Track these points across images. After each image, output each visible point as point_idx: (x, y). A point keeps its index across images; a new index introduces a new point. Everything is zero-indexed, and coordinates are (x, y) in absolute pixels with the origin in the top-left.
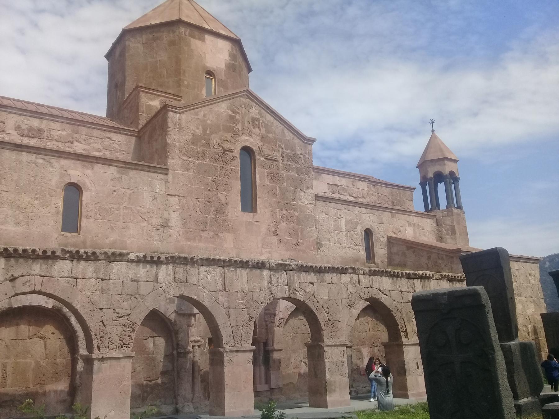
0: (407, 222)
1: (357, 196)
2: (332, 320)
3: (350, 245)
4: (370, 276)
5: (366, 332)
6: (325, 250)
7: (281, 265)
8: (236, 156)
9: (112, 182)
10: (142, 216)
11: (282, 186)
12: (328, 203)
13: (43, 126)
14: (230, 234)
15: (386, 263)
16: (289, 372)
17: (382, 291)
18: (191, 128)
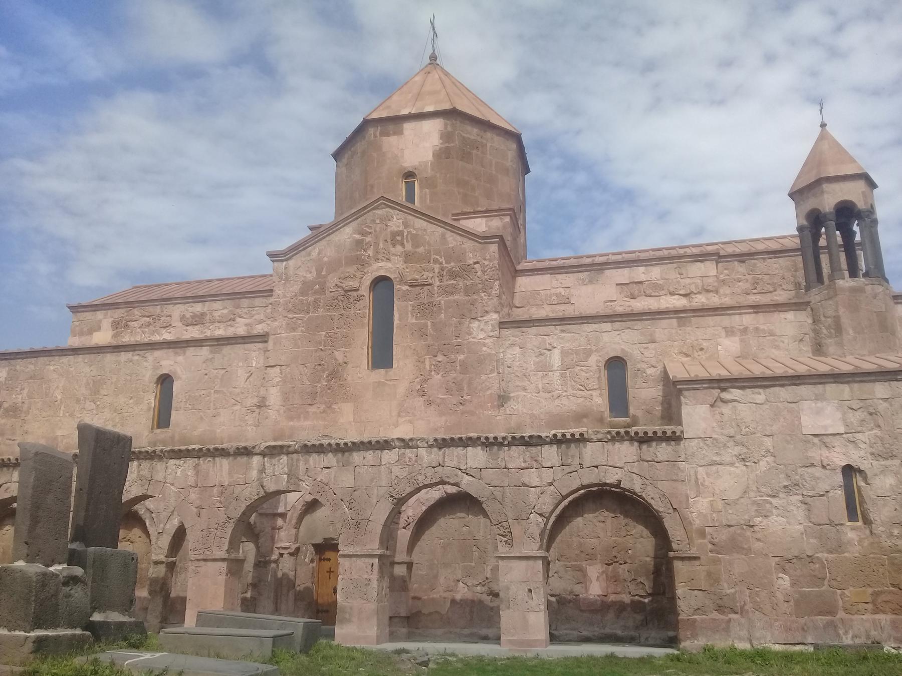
0: (725, 328)
1: (689, 292)
2: (357, 519)
3: (570, 391)
4: (440, 448)
5: (599, 537)
6: (515, 406)
7: (274, 447)
9: (205, 365)
12: (524, 329)
13: (205, 310)
14: (349, 404)
16: (435, 596)
17: (463, 471)
18: (301, 274)
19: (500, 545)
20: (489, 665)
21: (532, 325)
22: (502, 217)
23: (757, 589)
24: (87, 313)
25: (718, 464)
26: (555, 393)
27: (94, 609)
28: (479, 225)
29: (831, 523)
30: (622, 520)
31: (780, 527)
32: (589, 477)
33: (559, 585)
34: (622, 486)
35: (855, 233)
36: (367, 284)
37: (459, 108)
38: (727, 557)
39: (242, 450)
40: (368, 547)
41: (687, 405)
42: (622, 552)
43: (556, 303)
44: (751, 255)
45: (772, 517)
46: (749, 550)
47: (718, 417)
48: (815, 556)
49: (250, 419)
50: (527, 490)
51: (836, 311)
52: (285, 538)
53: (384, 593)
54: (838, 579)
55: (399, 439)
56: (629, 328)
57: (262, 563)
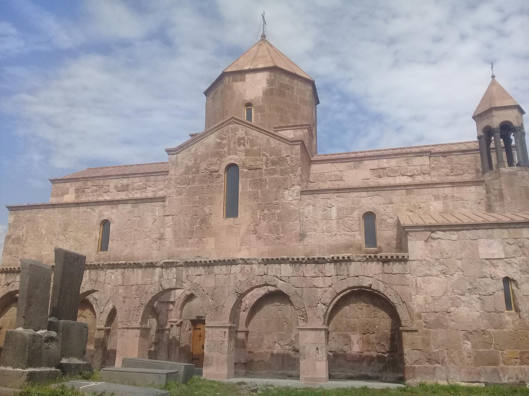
0: (434, 195)
1: (413, 174)
3: (342, 232)
4: (265, 265)
5: (358, 318)
7: (168, 263)
8: (221, 174)
9: (128, 214)
10: (146, 234)
11: (265, 189)
13: (129, 182)
15: (393, 245)
16: (261, 351)
17: (279, 278)
18: (185, 162)
19: (300, 322)
20: (293, 392)
21: (320, 193)
22: (303, 130)
23: (452, 350)
24: (60, 184)
25: (429, 276)
26: (333, 233)
27: (63, 356)
28: (289, 134)
29: (496, 311)
30: (372, 308)
31: (466, 313)
32: (353, 283)
33: (334, 346)
34: (372, 288)
35: (512, 140)
36: (224, 168)
37: (278, 65)
38: (434, 331)
39: (150, 264)
40: (223, 322)
41: (411, 240)
42: (372, 327)
43: (334, 180)
44: (450, 153)
45: (461, 307)
46: (447, 326)
47: (429, 248)
48: (486, 330)
49: (154, 246)
50: (316, 289)
51: (500, 186)
52: (174, 316)
53: (231, 349)
54: (500, 344)
55: (241, 259)
56: (378, 195)
57: (160, 331)
